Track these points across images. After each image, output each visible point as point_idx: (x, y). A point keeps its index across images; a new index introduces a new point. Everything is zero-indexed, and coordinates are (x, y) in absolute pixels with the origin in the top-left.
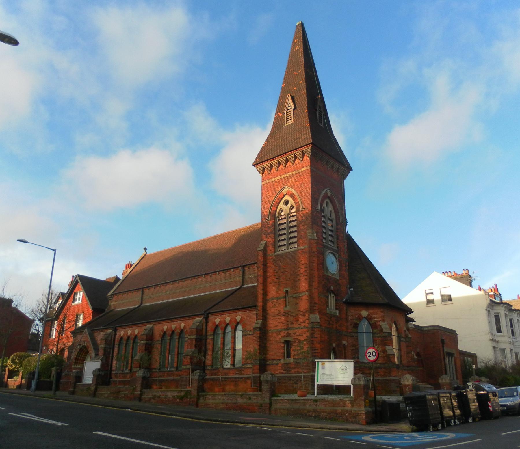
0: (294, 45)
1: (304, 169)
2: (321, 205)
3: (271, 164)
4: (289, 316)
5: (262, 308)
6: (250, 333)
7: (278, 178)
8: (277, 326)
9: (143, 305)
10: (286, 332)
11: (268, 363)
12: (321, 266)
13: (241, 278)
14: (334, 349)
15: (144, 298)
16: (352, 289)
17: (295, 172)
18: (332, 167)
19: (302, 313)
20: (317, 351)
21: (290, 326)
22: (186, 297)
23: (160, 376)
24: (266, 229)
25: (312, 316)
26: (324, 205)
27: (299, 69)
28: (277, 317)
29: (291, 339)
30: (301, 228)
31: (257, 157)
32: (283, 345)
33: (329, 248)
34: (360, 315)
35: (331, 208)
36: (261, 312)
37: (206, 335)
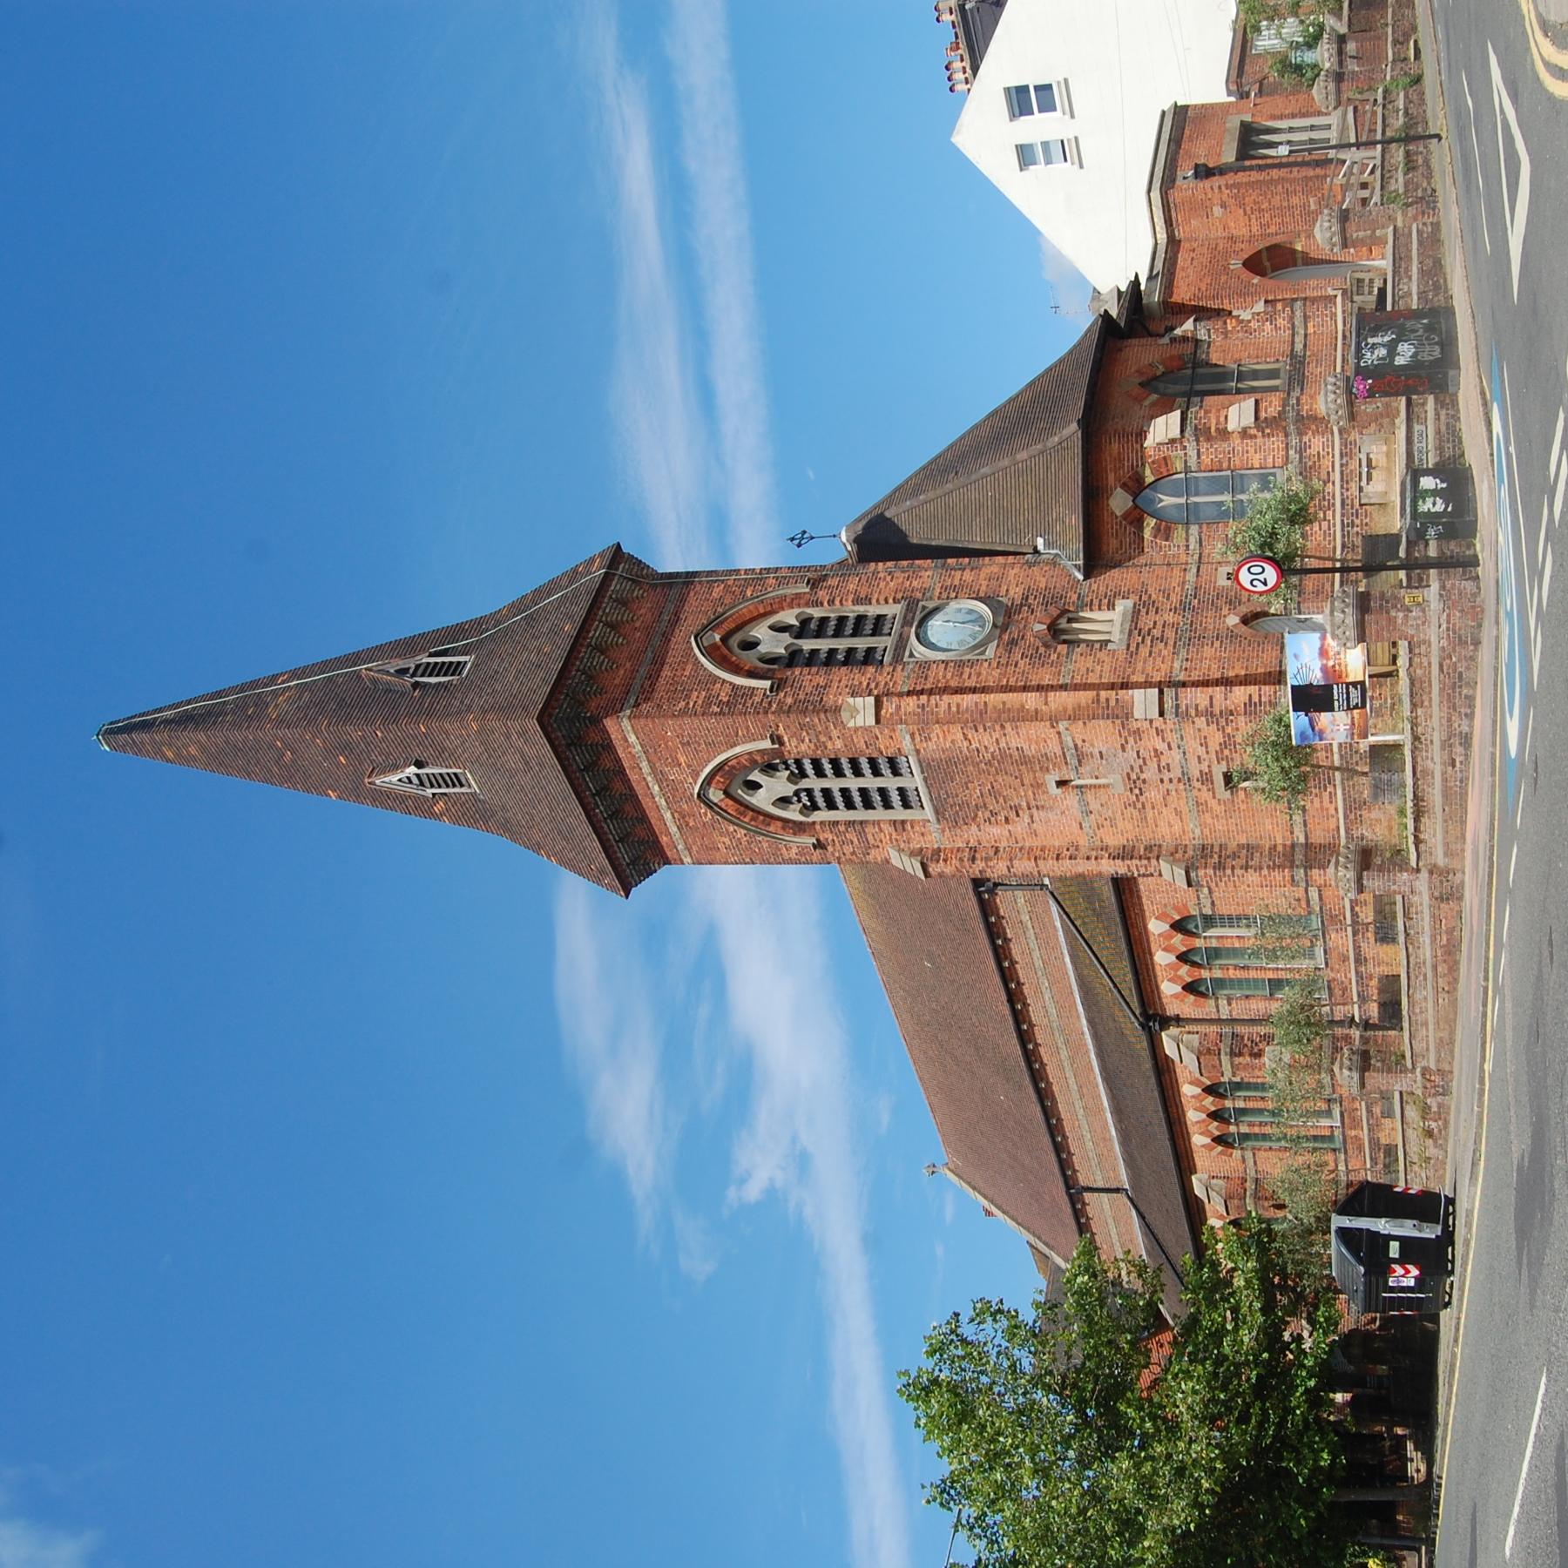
0: (183, 759)
1: (632, 738)
2: (752, 674)
3: (621, 840)
4: (1143, 776)
6: (1206, 890)
7: (668, 816)
8: (1178, 813)
9: (1127, 1186)
10: (1198, 785)
11: (1302, 840)
12: (967, 670)
13: (1019, 893)
14: (1246, 621)
15: (1100, 1184)
17: (644, 765)
18: (613, 626)
19: (1131, 740)
20: (1256, 699)
21: (1176, 773)
22: (1093, 1056)
23: (1360, 1148)
24: (848, 849)
25: (1138, 713)
26: (750, 659)
27: (272, 746)
28: (1150, 814)
29: (1218, 771)
30: (839, 744)
31: (599, 882)
32: (1242, 794)
34: (1126, 516)
35: (761, 632)
36: (1135, 862)
37: (1219, 1021)
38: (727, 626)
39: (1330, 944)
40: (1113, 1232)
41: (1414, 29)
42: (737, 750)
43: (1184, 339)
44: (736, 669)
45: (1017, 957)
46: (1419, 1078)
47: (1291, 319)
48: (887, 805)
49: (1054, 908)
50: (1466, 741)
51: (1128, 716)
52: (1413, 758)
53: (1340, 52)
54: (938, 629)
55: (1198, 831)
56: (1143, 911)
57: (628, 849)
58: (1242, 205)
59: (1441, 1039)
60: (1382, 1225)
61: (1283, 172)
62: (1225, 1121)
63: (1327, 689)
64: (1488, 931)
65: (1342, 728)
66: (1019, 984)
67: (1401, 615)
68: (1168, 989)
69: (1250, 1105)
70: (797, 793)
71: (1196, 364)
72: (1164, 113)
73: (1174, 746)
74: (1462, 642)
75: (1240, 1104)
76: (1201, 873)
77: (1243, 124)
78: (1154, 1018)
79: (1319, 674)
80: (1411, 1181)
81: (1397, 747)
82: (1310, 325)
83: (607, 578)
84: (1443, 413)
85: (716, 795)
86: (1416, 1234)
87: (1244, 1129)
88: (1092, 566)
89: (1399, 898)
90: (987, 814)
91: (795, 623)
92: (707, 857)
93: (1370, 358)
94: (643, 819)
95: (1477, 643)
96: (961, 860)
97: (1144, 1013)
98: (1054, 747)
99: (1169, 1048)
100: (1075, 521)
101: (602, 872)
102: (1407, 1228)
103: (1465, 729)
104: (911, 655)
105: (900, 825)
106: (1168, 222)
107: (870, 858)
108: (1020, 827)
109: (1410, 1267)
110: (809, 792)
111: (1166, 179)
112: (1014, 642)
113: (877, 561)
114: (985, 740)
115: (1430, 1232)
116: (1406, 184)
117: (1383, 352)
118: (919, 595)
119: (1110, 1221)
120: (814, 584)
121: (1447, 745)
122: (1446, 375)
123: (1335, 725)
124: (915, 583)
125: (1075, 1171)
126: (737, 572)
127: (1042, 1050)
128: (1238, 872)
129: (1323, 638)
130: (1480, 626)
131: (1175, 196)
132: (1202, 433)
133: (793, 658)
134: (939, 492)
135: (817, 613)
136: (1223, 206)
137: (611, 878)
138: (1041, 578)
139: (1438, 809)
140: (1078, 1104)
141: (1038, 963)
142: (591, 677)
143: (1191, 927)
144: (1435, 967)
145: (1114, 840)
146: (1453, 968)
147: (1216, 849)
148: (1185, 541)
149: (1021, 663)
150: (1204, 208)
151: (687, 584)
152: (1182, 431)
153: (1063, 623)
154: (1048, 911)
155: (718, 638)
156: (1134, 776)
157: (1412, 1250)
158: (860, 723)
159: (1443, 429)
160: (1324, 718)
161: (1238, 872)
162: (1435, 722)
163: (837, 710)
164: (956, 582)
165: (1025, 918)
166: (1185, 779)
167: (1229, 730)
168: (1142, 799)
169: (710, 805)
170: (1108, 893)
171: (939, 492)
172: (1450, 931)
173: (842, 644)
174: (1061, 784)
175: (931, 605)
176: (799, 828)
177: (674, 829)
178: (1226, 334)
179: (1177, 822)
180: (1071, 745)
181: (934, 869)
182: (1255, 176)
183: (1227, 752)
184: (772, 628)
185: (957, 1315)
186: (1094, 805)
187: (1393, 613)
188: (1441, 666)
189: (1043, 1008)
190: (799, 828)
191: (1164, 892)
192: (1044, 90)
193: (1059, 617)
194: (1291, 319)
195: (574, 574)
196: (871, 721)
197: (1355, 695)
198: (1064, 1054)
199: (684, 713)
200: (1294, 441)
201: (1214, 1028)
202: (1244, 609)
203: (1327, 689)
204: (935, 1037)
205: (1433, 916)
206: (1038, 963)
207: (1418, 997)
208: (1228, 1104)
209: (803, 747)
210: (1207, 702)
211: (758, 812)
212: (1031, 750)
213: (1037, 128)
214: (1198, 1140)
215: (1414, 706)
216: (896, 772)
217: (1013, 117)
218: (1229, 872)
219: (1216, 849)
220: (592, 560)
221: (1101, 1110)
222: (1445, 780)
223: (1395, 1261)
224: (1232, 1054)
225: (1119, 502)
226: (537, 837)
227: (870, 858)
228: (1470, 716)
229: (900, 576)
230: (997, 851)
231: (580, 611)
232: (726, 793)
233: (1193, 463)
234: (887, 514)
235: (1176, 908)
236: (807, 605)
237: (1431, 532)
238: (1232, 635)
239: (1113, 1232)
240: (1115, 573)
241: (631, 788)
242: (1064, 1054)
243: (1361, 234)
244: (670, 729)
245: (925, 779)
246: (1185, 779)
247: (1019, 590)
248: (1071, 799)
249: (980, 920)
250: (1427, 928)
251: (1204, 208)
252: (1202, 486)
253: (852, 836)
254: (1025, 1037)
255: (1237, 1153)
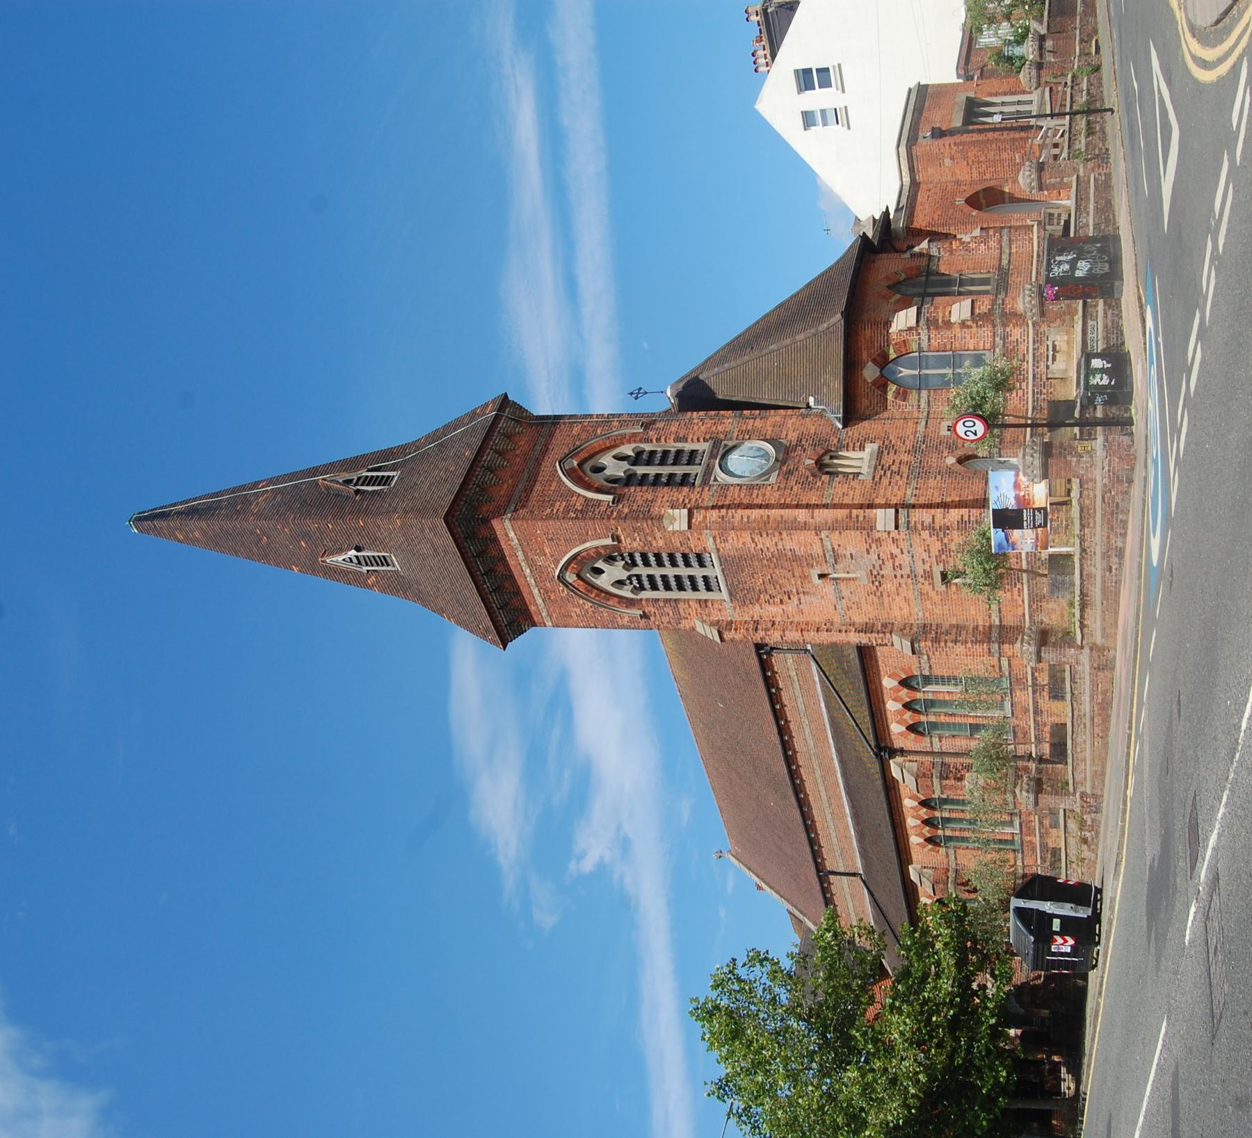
1: (512, 534)
2: (599, 490)
3: (502, 608)
5: (862, 635)
7: (536, 591)
8: (907, 600)
10: (922, 580)
11: (997, 622)
13: (789, 655)
14: (960, 461)
15: (842, 870)
16: (811, 400)
17: (520, 554)
18: (501, 453)
19: (874, 546)
20: (966, 518)
21: (906, 571)
22: (839, 776)
23: (1034, 849)
24: (665, 619)
25: (880, 527)
26: (598, 479)
28: (886, 599)
30: (661, 543)
31: (484, 637)
32: (954, 588)
33: (709, 471)
34: (874, 383)
36: (874, 635)
38: (583, 455)
39: (1016, 699)
40: (850, 905)
41: (1095, 31)
42: (588, 545)
43: (921, 254)
44: (588, 487)
45: (786, 702)
46: (1078, 800)
47: (1000, 242)
48: (695, 588)
49: (814, 666)
50: (1120, 553)
51: (872, 528)
52: (1081, 565)
53: (1041, 48)
54: (734, 460)
55: (920, 614)
56: (878, 670)
57: (507, 616)
58: (966, 158)
59: (1096, 772)
60: (1048, 907)
61: (997, 135)
62: (935, 826)
63: (1019, 513)
64: (1133, 693)
65: (1029, 541)
66: (786, 721)
67: (1075, 459)
68: (896, 728)
69: (954, 815)
70: (629, 578)
71: (929, 273)
72: (910, 90)
73: (905, 551)
74: (1120, 481)
75: (946, 815)
76: (922, 644)
77: (968, 99)
78: (884, 750)
79: (1013, 501)
80: (1071, 875)
81: (1068, 556)
82: (1013, 246)
83: (497, 418)
84: (1110, 312)
85: (571, 577)
86: (1073, 914)
87: (948, 833)
88: (850, 416)
89: (1067, 667)
90: (767, 597)
91: (632, 454)
92: (564, 621)
93: (1057, 271)
94: (518, 592)
95: (1130, 481)
96: (747, 630)
97: (878, 746)
98: (817, 549)
99: (895, 771)
100: (837, 386)
101: (487, 630)
102: (1067, 910)
103: (1120, 544)
104: (715, 480)
105: (703, 603)
106: (912, 169)
107: (681, 626)
108: (791, 607)
109: (1067, 938)
110: (639, 577)
111: (910, 138)
112: (790, 472)
113: (692, 411)
114: (767, 543)
115: (1084, 913)
116: (1087, 145)
117: (1067, 267)
118: (722, 436)
119: (848, 897)
120: (647, 426)
121: (1106, 556)
122: (1113, 285)
123: (1024, 539)
124: (720, 428)
125: (823, 859)
126: (591, 416)
127: (802, 770)
128: (950, 644)
129: (1017, 475)
130: (1133, 469)
131: (917, 150)
132: (932, 324)
133: (630, 479)
134: (739, 362)
135: (648, 447)
136: (952, 158)
137: (493, 635)
138: (811, 426)
139: (1098, 603)
140: (828, 811)
141: (801, 707)
142: (483, 490)
143: (914, 684)
144: (1092, 719)
145: (859, 619)
146: (1106, 720)
147: (934, 627)
148: (918, 402)
149: (795, 488)
150: (937, 159)
151: (555, 424)
152: (918, 322)
153: (826, 460)
154: (810, 670)
155: (575, 463)
156: (875, 572)
157: (1070, 926)
158: (677, 528)
159: (1110, 324)
160: (1016, 534)
161: (950, 644)
162: (1098, 539)
163: (661, 518)
164: (750, 428)
165: (793, 674)
166: (912, 575)
167: (946, 541)
168: (881, 589)
169: (566, 584)
170: (854, 656)
171: (739, 362)
172: (1105, 693)
173: (665, 470)
174: (822, 576)
175: (731, 444)
176: (630, 603)
177: (540, 601)
178: (951, 252)
179: (906, 606)
180: (830, 548)
181: (727, 636)
182: (976, 137)
183: (944, 557)
184: (615, 457)
185: (734, 960)
186: (846, 593)
187: (1069, 458)
188: (1103, 498)
189: (803, 740)
190: (630, 603)
191: (895, 657)
192: (823, 72)
193: (823, 455)
194: (1000, 242)
195: (473, 415)
196: (685, 527)
197: (1039, 518)
198: (818, 773)
199: (549, 517)
200: (999, 330)
201: (929, 759)
202: (959, 453)
203: (1019, 513)
204: (725, 758)
205: (1092, 681)
206: (801, 707)
207: (1079, 740)
208: (937, 814)
209: (635, 545)
210: (930, 520)
211: (601, 590)
212: (800, 551)
213: (818, 99)
214: (915, 840)
215: (1082, 527)
216: (702, 565)
217: (800, 91)
218: (942, 644)
219: (934, 627)
220: (487, 405)
221: (845, 815)
222: (1104, 582)
223: (1057, 933)
224: (942, 778)
225: (870, 372)
226: (441, 603)
227: (681, 626)
228: (1124, 535)
229: (709, 422)
230: (774, 624)
231: (476, 442)
232: (578, 576)
233: (925, 345)
234: (701, 377)
235: (903, 670)
236: (641, 441)
237: (1099, 399)
238: (950, 471)
239: (850, 905)
240: (866, 424)
241: (510, 571)
242: (818, 773)
243: (1053, 180)
244: (539, 528)
245: (723, 570)
246: (912, 575)
247: (795, 435)
248: (828, 588)
249: (760, 673)
250: (1087, 690)
251: (937, 159)
252: (931, 362)
253: (668, 610)
254: (790, 760)
255: (942, 850)
